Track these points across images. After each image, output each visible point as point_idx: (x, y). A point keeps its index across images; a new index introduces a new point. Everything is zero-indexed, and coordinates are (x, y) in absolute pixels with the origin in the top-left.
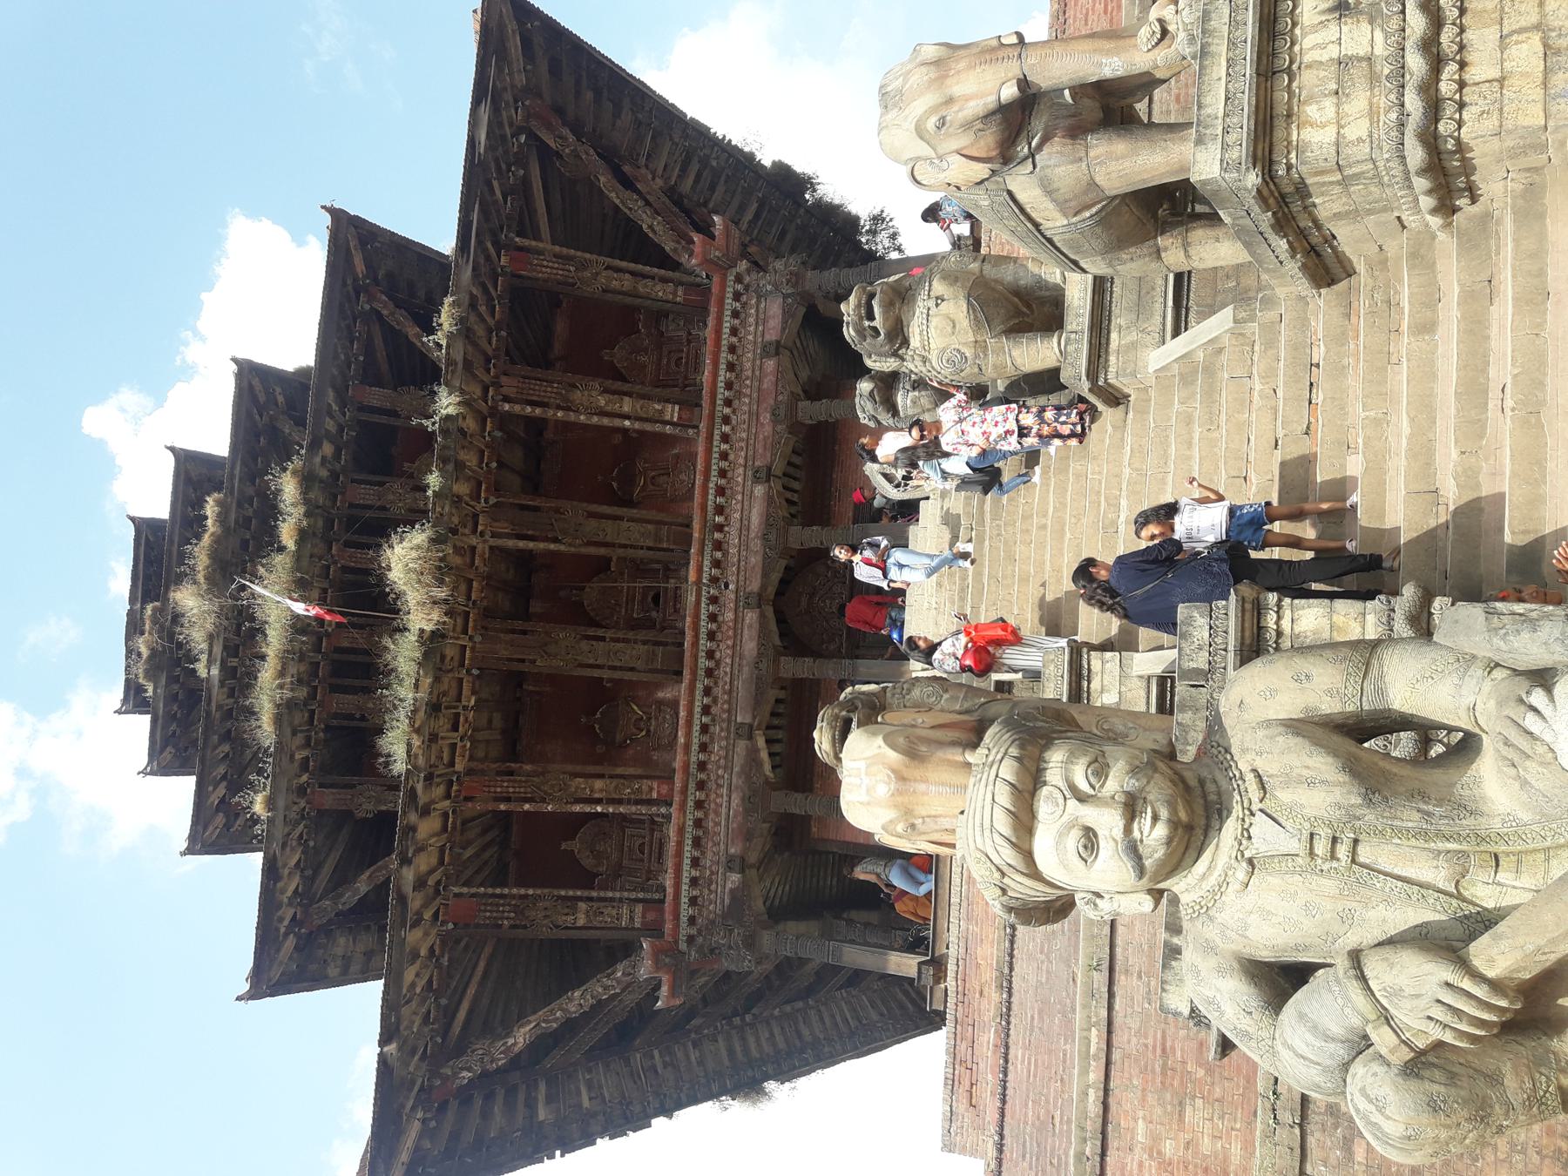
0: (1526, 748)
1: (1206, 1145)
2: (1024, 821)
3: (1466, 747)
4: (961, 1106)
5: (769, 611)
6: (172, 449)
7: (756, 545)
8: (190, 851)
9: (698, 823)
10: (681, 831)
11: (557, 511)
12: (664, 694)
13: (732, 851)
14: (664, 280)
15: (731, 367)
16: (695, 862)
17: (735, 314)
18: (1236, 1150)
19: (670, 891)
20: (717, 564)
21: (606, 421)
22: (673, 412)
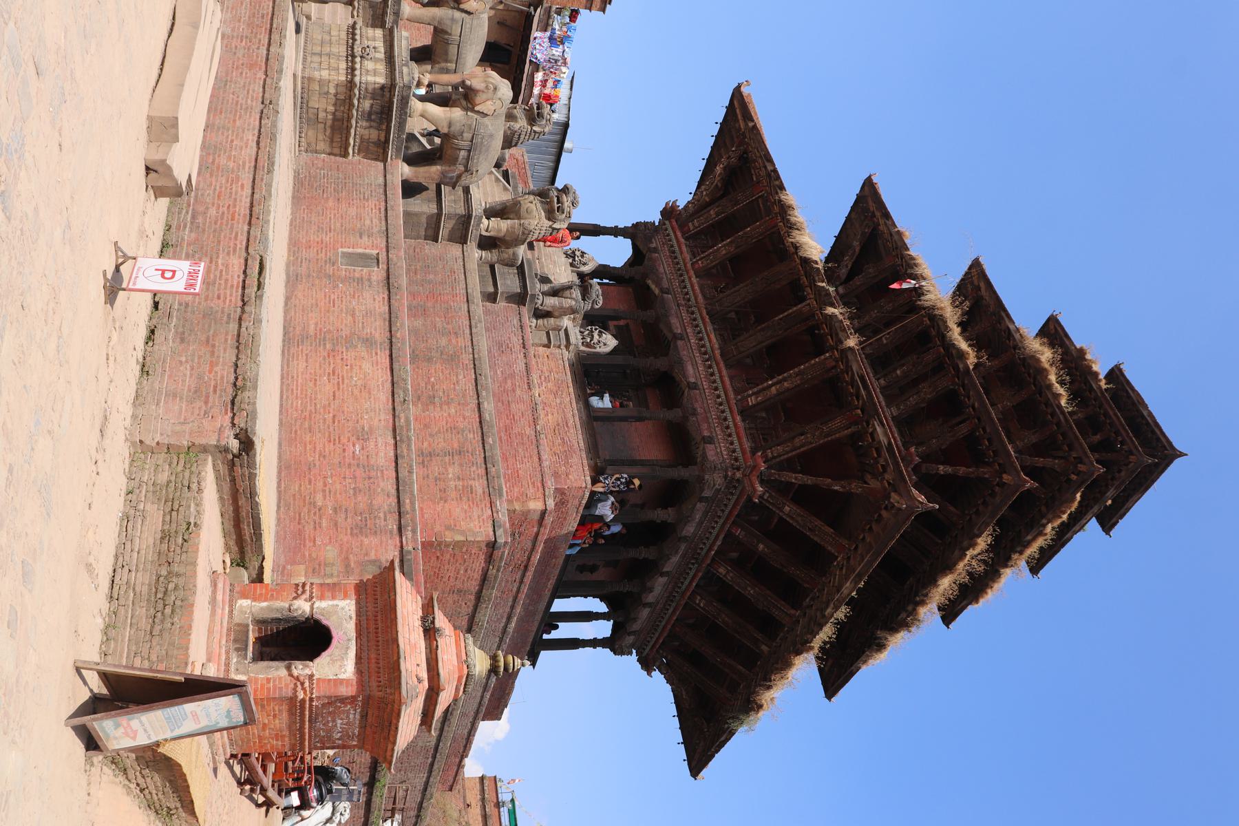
5: (669, 336)
10: (681, 253)
15: (728, 427)
17: (734, 451)
20: (703, 346)
22: (752, 401)
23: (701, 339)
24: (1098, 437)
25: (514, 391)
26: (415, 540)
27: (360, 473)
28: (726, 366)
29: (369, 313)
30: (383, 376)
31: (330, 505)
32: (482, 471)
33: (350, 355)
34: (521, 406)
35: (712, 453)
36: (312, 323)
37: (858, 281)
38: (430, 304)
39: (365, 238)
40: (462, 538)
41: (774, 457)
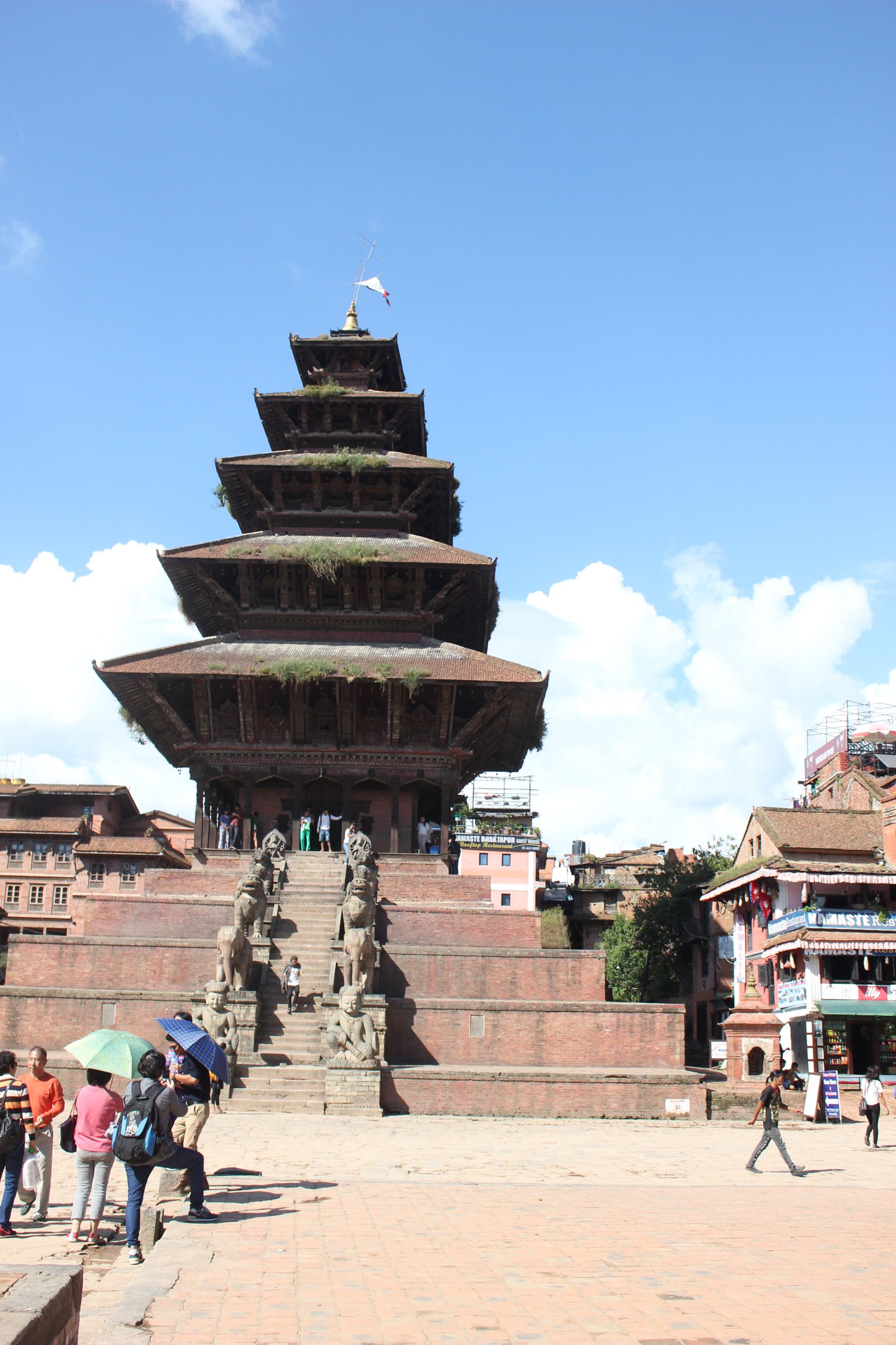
1: (167, 970)
2: (215, 992)
6: (423, 393)
7: (344, 772)
8: (217, 464)
9: (240, 755)
11: (352, 701)
12: (287, 736)
13: (231, 768)
14: (448, 731)
15: (414, 758)
16: (225, 754)
17: (435, 759)
18: (167, 976)
19: (215, 745)
20: (337, 757)
21: (389, 715)
22: (396, 736)
23: (330, 756)
24: (380, 413)
26: (657, 1007)
27: (621, 1029)
28: (355, 744)
29: (518, 1021)
30: (562, 1017)
31: (639, 1044)
32: (562, 961)
33: (549, 1032)
34: (465, 921)
37: (244, 592)
38: (439, 979)
39: (460, 1022)
41: (448, 736)
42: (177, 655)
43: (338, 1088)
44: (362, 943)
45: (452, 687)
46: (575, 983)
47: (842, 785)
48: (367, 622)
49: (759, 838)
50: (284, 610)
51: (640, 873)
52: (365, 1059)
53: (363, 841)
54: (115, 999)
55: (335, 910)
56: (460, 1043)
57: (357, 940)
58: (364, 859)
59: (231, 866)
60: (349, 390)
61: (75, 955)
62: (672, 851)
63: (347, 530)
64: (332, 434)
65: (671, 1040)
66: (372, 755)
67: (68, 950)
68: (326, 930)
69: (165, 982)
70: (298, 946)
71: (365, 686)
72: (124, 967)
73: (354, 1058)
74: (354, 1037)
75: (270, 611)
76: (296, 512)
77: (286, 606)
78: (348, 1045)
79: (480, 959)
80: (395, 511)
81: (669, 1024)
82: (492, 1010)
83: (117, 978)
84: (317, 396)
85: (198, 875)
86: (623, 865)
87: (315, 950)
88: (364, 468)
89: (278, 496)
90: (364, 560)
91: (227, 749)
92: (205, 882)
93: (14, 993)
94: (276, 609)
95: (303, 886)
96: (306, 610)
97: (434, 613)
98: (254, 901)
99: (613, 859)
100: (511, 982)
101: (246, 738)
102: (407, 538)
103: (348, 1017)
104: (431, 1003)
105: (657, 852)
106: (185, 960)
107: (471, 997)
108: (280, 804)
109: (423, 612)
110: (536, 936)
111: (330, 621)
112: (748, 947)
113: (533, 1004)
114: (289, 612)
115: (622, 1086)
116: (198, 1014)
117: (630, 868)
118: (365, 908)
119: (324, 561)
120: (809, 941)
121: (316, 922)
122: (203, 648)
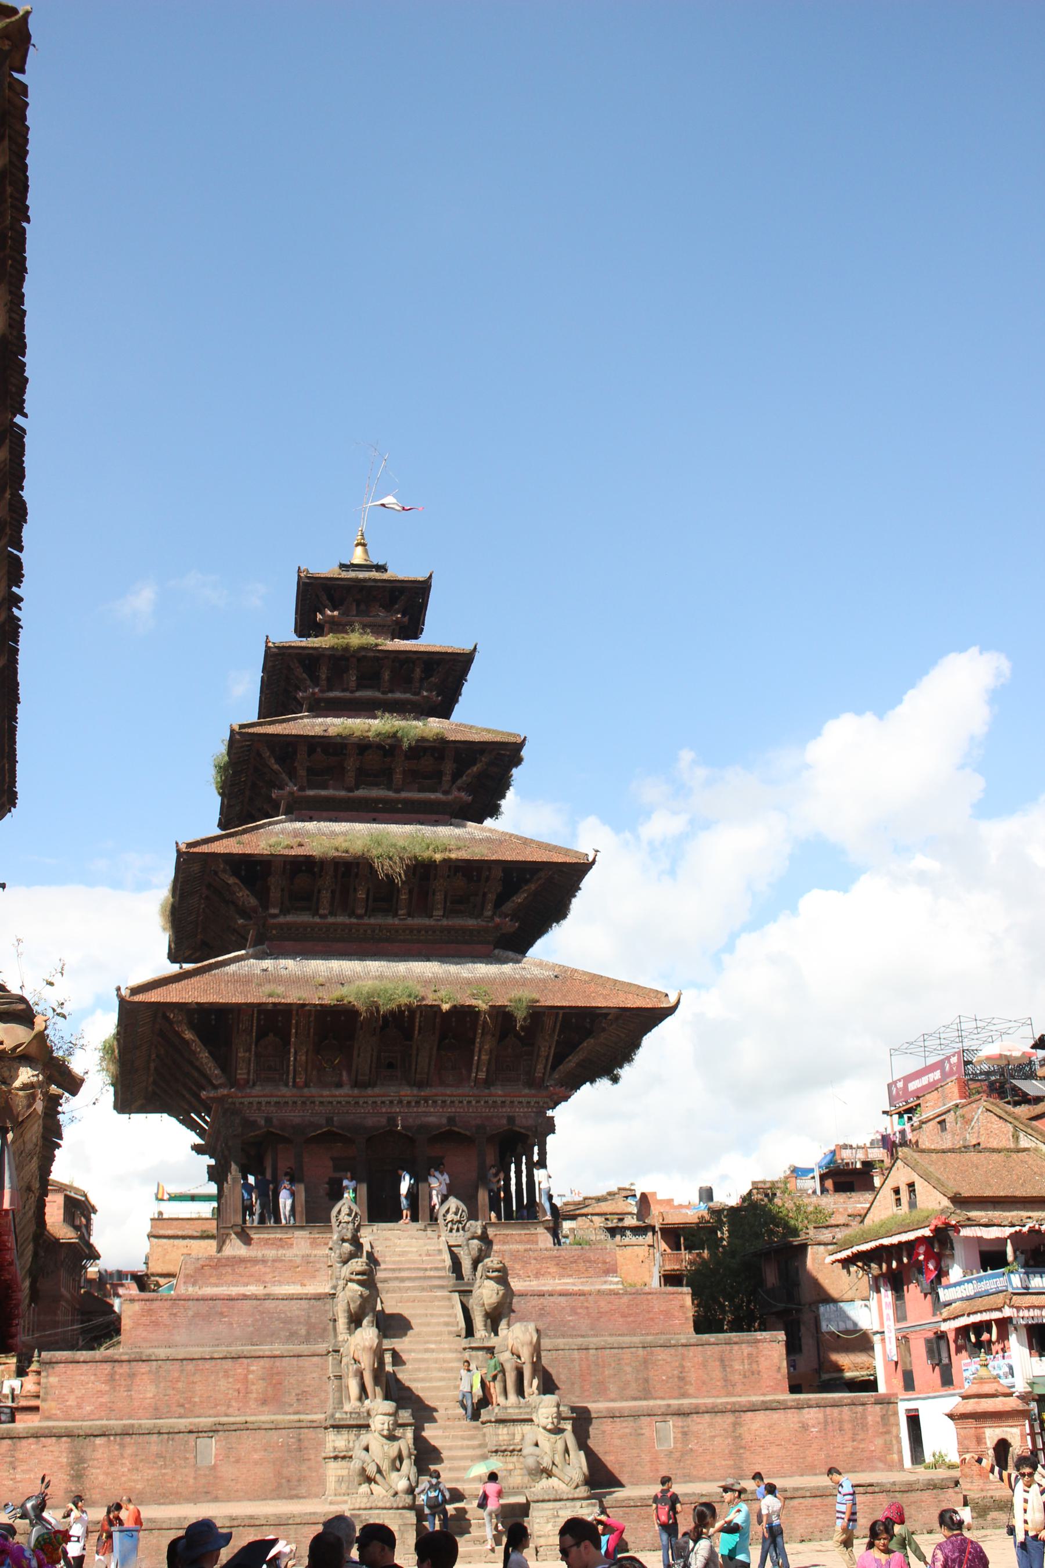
0: (401, 1477)
1: (254, 1387)
2: (385, 1414)
3: (398, 1470)
4: (201, 1262)
7: (418, 1122)
8: (232, 731)
9: (287, 1103)
10: (283, 1096)
12: (345, 1076)
13: (274, 1120)
14: (545, 1068)
17: (528, 1103)
18: (254, 1395)
20: (409, 1103)
21: (477, 1049)
22: (482, 1075)
24: (418, 670)
25: (587, 1308)
26: (868, 1397)
27: (830, 1427)
29: (711, 1425)
30: (761, 1415)
32: (736, 1347)
33: (748, 1437)
34: (602, 1304)
35: (524, 1120)
36: (724, 1463)
37: (275, 894)
39: (643, 1431)
40: (785, 1364)
42: (206, 976)
43: (550, 1526)
44: (535, 1340)
45: (557, 1014)
46: (753, 1373)
47: (963, 1116)
48: (427, 932)
49: (911, 1185)
50: (322, 916)
51: (610, 1225)
52: (577, 1487)
53: (458, 1209)
54: (213, 1431)
55: (450, 1299)
56: (646, 1458)
57: (527, 1338)
58: (479, 1232)
59: (282, 1247)
60: (379, 641)
61: (132, 1376)
62: (644, 1196)
63: (387, 816)
64: (358, 694)
65: (887, 1436)
66: (452, 1099)
67: (124, 1369)
68: (447, 1324)
69: (253, 1405)
70: (422, 1347)
71: (464, 1014)
72: (198, 1388)
73: (563, 1486)
74: (558, 1459)
75: (305, 918)
76: (323, 793)
77: (326, 912)
78: (555, 1470)
79: (641, 1352)
80: (446, 793)
81: (883, 1417)
82: (681, 1413)
83: (190, 1402)
84: (346, 648)
85: (254, 1261)
86: (586, 1215)
87: (443, 1350)
88: (418, 741)
89: (302, 773)
90: (438, 857)
91: (272, 1096)
92: (263, 1270)
93: (76, 1432)
94: (313, 916)
95: (400, 1269)
96: (350, 916)
97: (511, 920)
98: (366, 1293)
99: (572, 1207)
100: (679, 1377)
101: (294, 1081)
102: (464, 826)
103: (547, 1434)
104: (608, 1409)
105: (627, 1197)
106: (278, 1373)
107: (635, 1399)
108: (331, 1164)
109: (497, 920)
110: (687, 1318)
111: (381, 930)
112: (900, 1315)
113: (727, 1403)
114: (331, 920)
115: (869, 1497)
116: (364, 1443)
117: (595, 1218)
118: (504, 1294)
119: (391, 858)
120: (1018, 1308)
121: (432, 1315)
122: (232, 968)
